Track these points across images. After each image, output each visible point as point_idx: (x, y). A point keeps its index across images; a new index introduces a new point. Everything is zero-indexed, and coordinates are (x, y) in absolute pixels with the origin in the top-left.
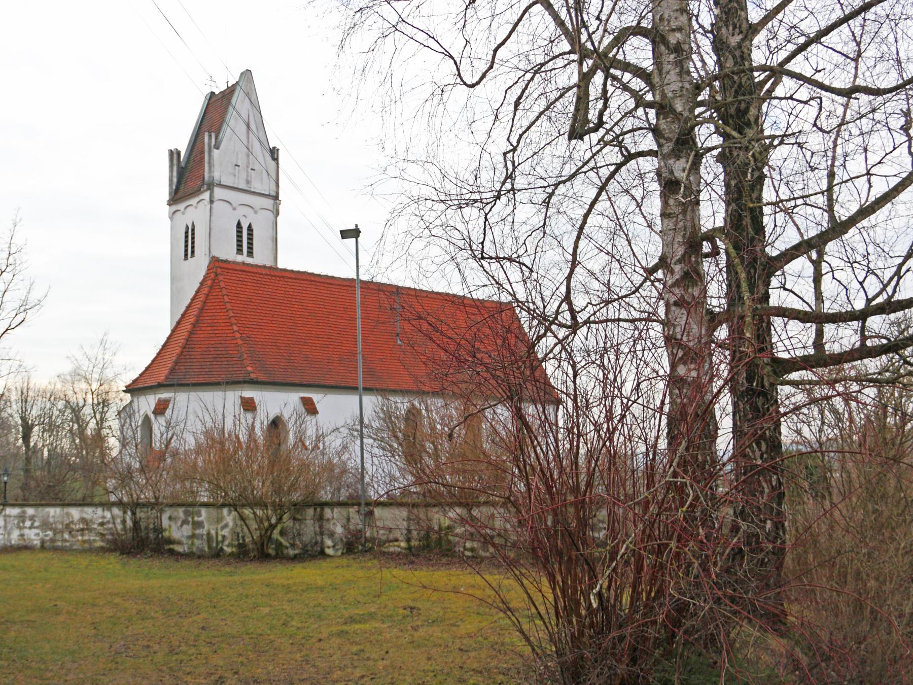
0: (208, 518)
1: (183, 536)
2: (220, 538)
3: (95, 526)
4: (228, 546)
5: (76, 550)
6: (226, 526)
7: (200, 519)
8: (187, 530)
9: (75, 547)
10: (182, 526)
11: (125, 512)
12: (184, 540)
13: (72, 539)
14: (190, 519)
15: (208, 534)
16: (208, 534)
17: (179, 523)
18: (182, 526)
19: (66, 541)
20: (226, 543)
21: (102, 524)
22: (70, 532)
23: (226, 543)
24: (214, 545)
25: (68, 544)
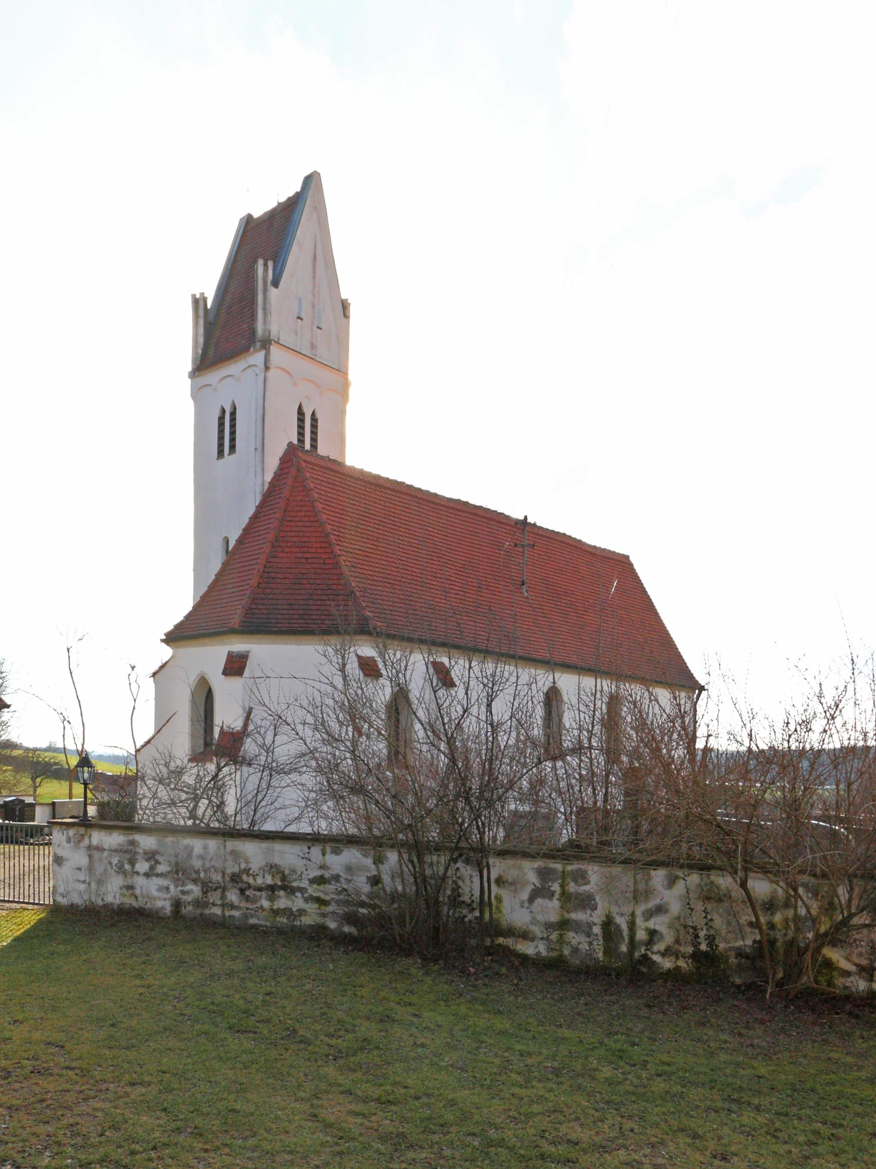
0: (607, 889)
1: (534, 921)
2: (641, 935)
3: (304, 884)
4: (663, 955)
5: (254, 927)
6: (660, 910)
7: (586, 888)
8: (550, 909)
9: (253, 921)
10: (531, 900)
11: (379, 860)
12: (537, 930)
13: (243, 904)
14: (556, 887)
15: (608, 924)
16: (608, 924)
17: (525, 895)
18: (531, 900)
19: (232, 907)
20: (660, 946)
21: (320, 881)
22: (242, 891)
23: (660, 946)
24: (624, 948)
25: (236, 913)
